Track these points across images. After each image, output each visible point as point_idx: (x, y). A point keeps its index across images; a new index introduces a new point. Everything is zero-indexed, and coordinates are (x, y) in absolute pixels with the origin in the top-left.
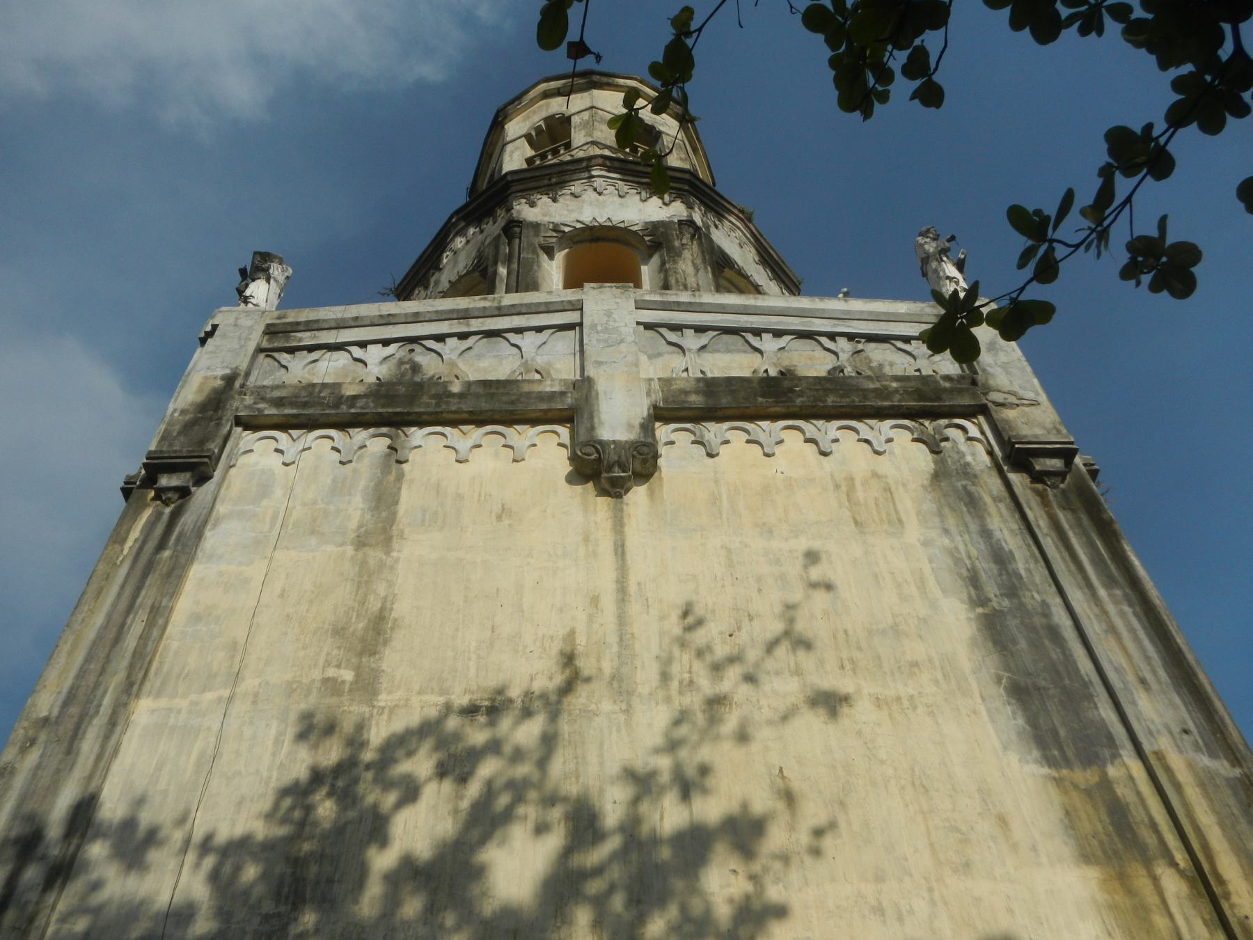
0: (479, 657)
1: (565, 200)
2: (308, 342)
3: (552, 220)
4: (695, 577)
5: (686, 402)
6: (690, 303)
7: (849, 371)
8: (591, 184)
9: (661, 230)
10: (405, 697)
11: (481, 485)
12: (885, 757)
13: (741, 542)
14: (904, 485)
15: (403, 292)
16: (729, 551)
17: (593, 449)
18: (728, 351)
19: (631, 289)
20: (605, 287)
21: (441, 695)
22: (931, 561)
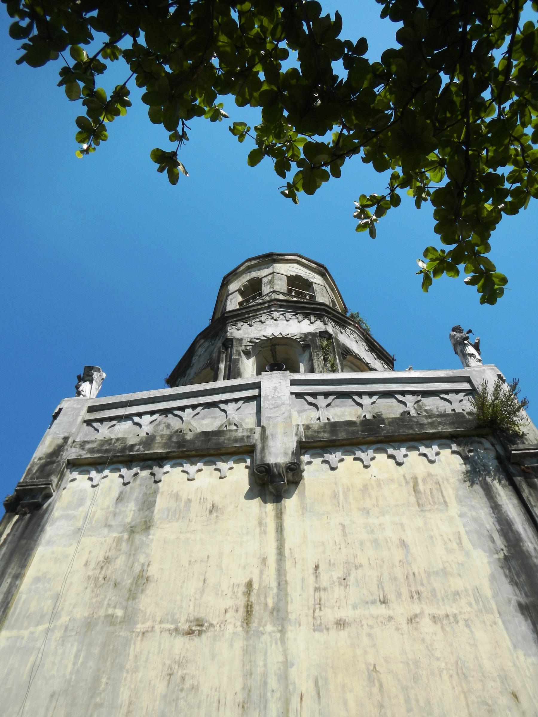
0: (195, 599)
1: (257, 325)
3: (250, 336)
4: (323, 543)
5: (319, 437)
7: (413, 413)
8: (271, 315)
10: (152, 626)
11: (201, 494)
12: (439, 656)
13: (351, 520)
14: (447, 480)
15: (172, 381)
16: (343, 526)
20: (274, 374)
21: (172, 624)
22: (465, 526)
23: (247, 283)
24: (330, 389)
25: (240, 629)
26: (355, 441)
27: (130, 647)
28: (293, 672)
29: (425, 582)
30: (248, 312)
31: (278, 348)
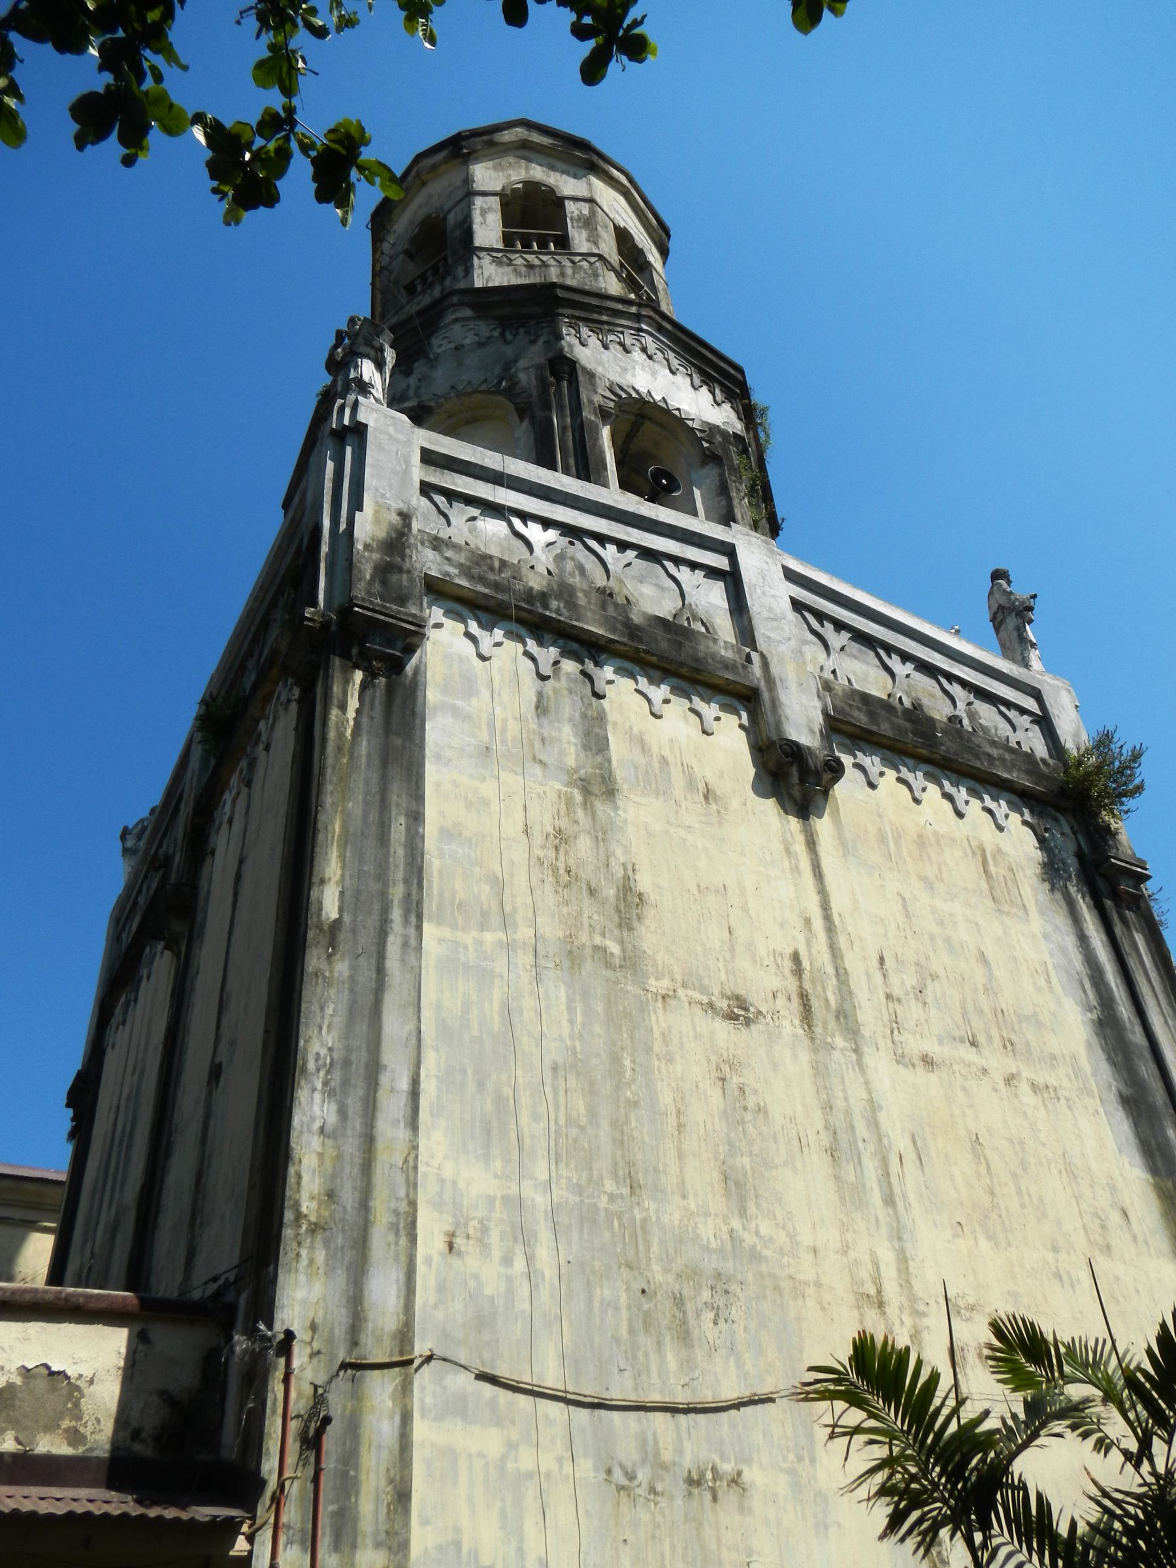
2: (446, 482)
14: (1023, 869)
23: (520, 186)
24: (843, 616)
25: (800, 1031)
26: (899, 745)
27: (649, 1016)
28: (882, 1116)
29: (1016, 1027)
30: (600, 310)
31: (648, 427)
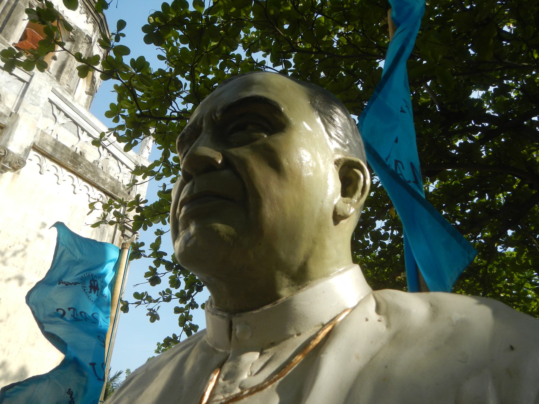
5: (45, 148)
6: (70, 103)
9: (79, 34)
17: (4, 151)
18: (70, 131)
19: (54, 81)
